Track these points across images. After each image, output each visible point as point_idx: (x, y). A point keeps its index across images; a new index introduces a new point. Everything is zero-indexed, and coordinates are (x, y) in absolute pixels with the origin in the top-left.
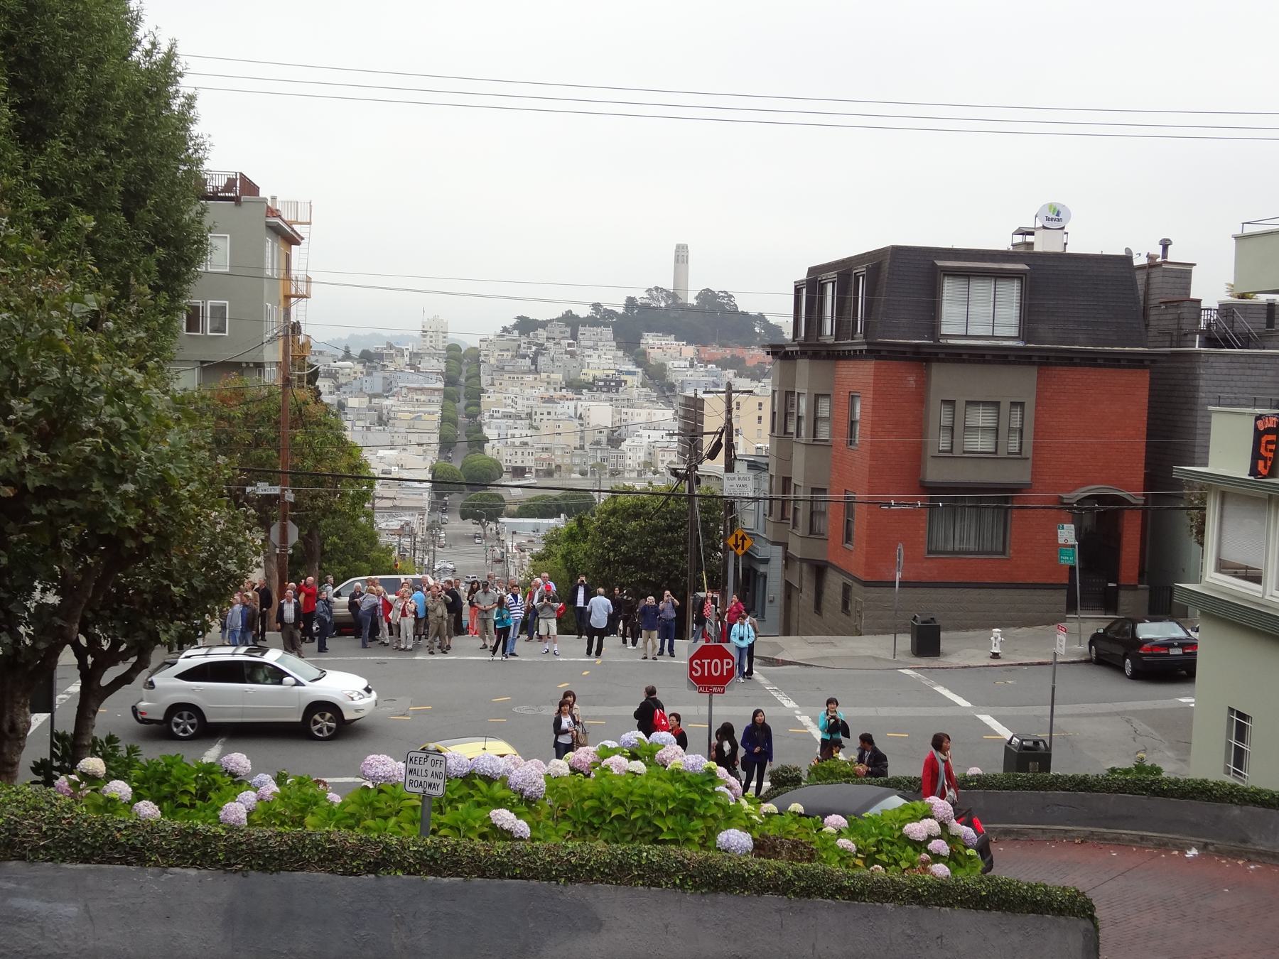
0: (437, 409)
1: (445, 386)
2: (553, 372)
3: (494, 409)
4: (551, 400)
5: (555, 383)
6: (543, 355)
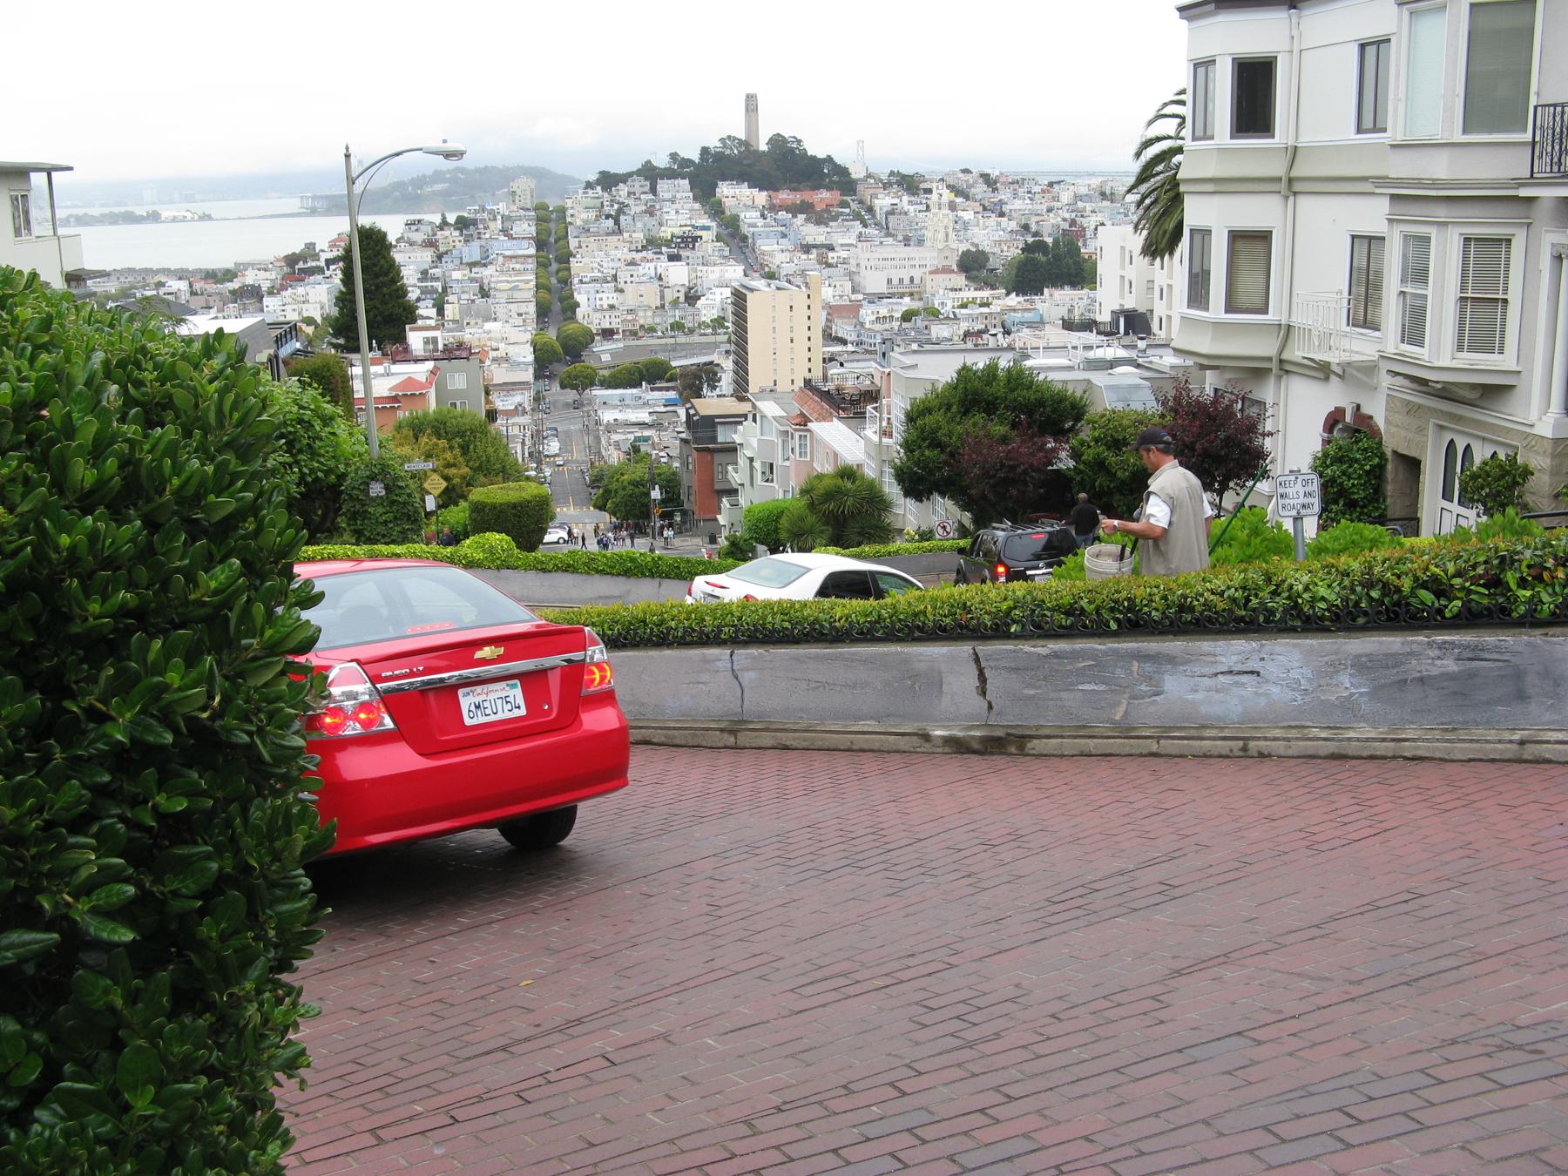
0: (532, 277)
1: (537, 251)
4: (632, 263)
5: (637, 242)
6: (624, 213)
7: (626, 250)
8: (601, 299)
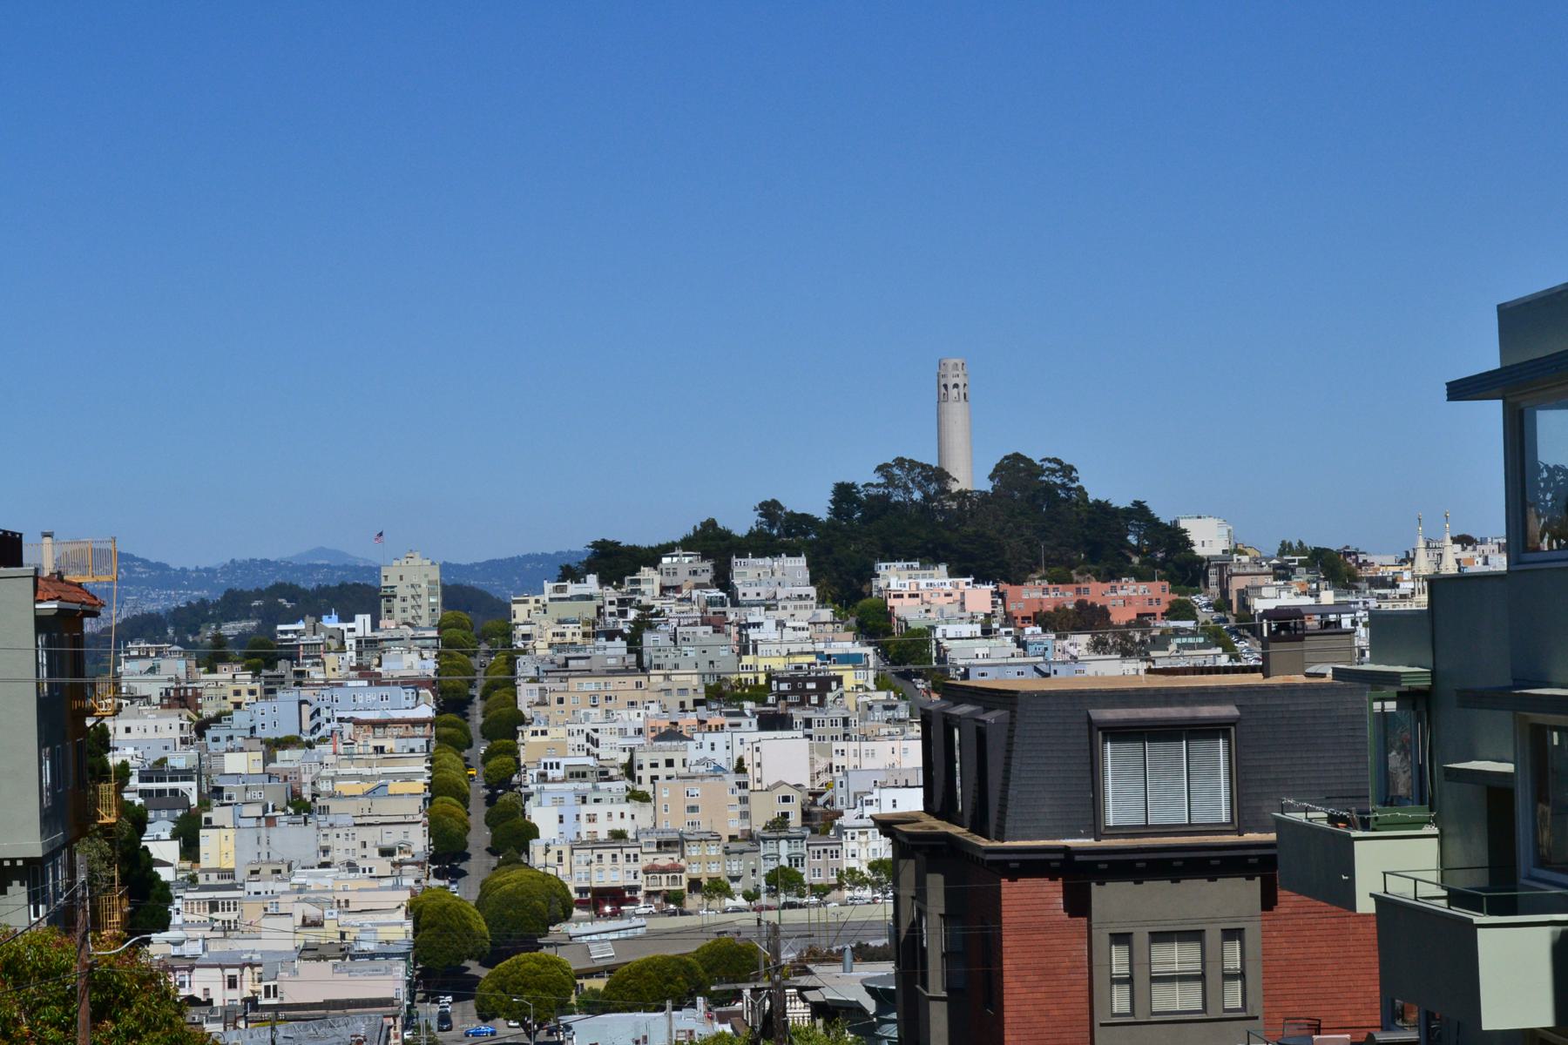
0: (420, 766)
2: (676, 667)
3: (548, 761)
4: (672, 734)
5: (683, 691)
6: (651, 627)
7: (654, 708)
8: (592, 819)
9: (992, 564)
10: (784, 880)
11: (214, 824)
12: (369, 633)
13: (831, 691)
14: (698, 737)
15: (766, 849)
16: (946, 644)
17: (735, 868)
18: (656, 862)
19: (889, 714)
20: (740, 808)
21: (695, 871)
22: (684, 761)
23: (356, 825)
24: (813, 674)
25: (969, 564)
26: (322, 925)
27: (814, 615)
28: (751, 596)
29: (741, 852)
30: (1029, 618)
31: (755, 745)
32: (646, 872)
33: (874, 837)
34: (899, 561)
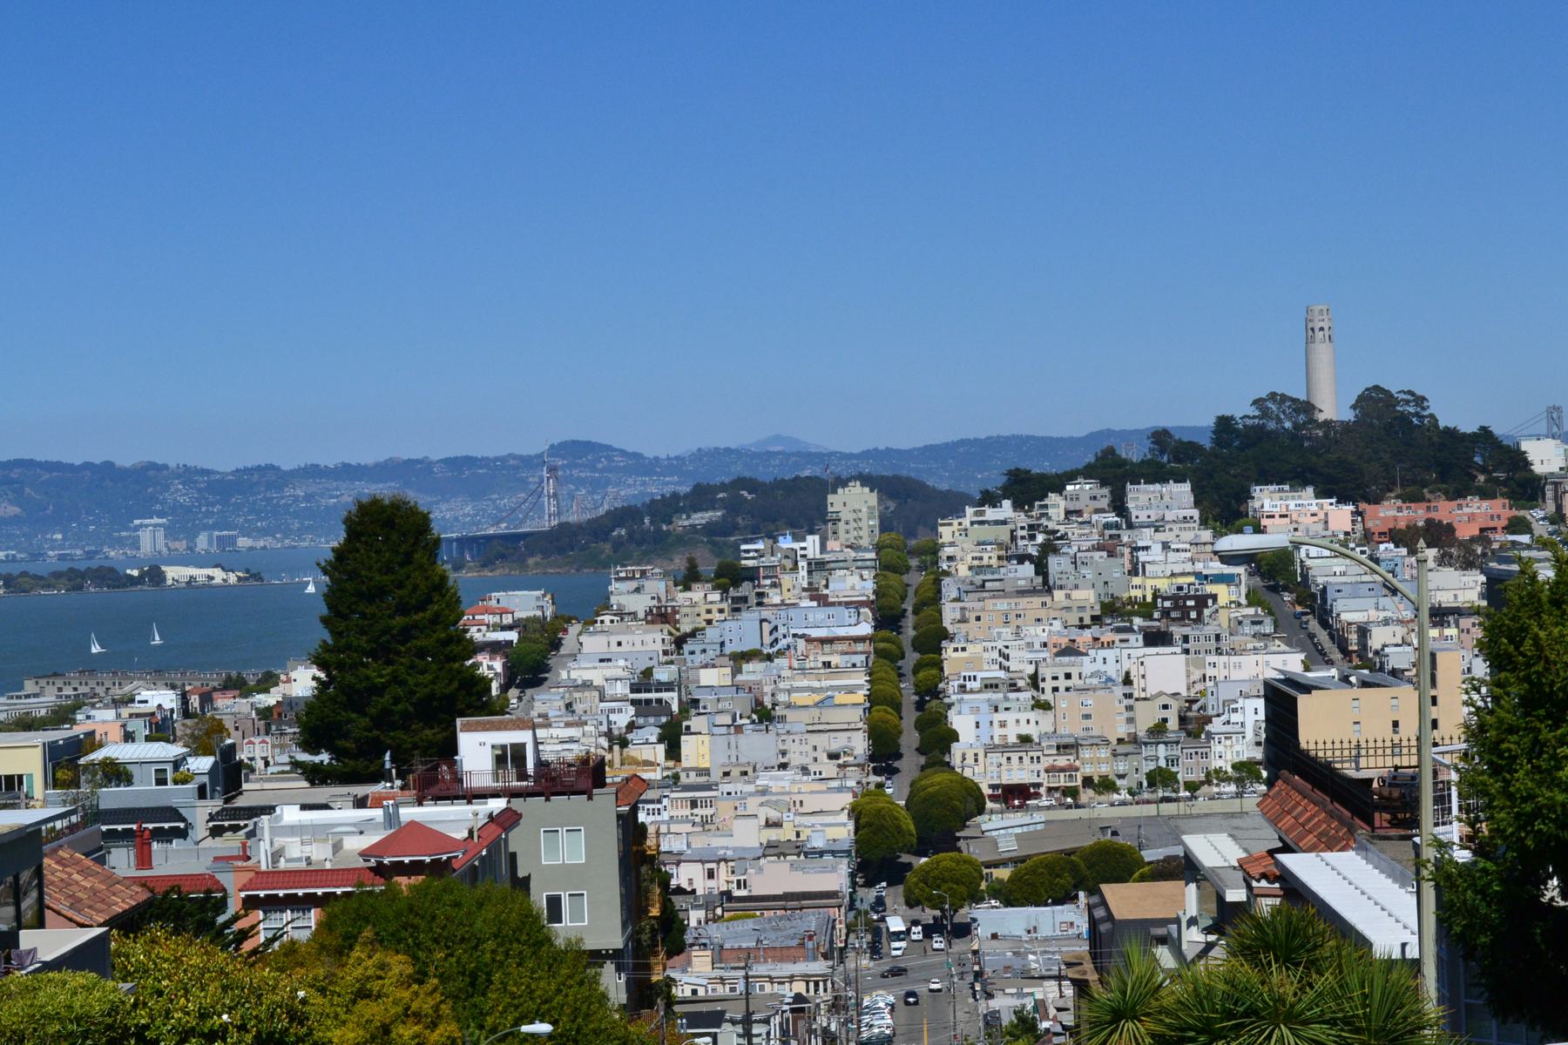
0: (861, 679)
2: (1076, 587)
3: (967, 674)
4: (1070, 650)
5: (1082, 608)
6: (1056, 551)
7: (1057, 625)
8: (1003, 724)
9: (1353, 486)
10: (1160, 778)
11: (692, 730)
12: (818, 556)
13: (1207, 607)
14: (1092, 652)
15: (1147, 751)
16: (1308, 563)
17: (1121, 768)
18: (1055, 763)
19: (1257, 628)
20: (1127, 714)
21: (1088, 770)
22: (1080, 674)
23: (808, 732)
24: (1192, 593)
25: (1334, 487)
26: (781, 826)
27: (1196, 536)
28: (1143, 518)
29: (1126, 755)
30: (1385, 533)
31: (1140, 660)
32: (1047, 771)
33: (1238, 741)
34: (1272, 484)
